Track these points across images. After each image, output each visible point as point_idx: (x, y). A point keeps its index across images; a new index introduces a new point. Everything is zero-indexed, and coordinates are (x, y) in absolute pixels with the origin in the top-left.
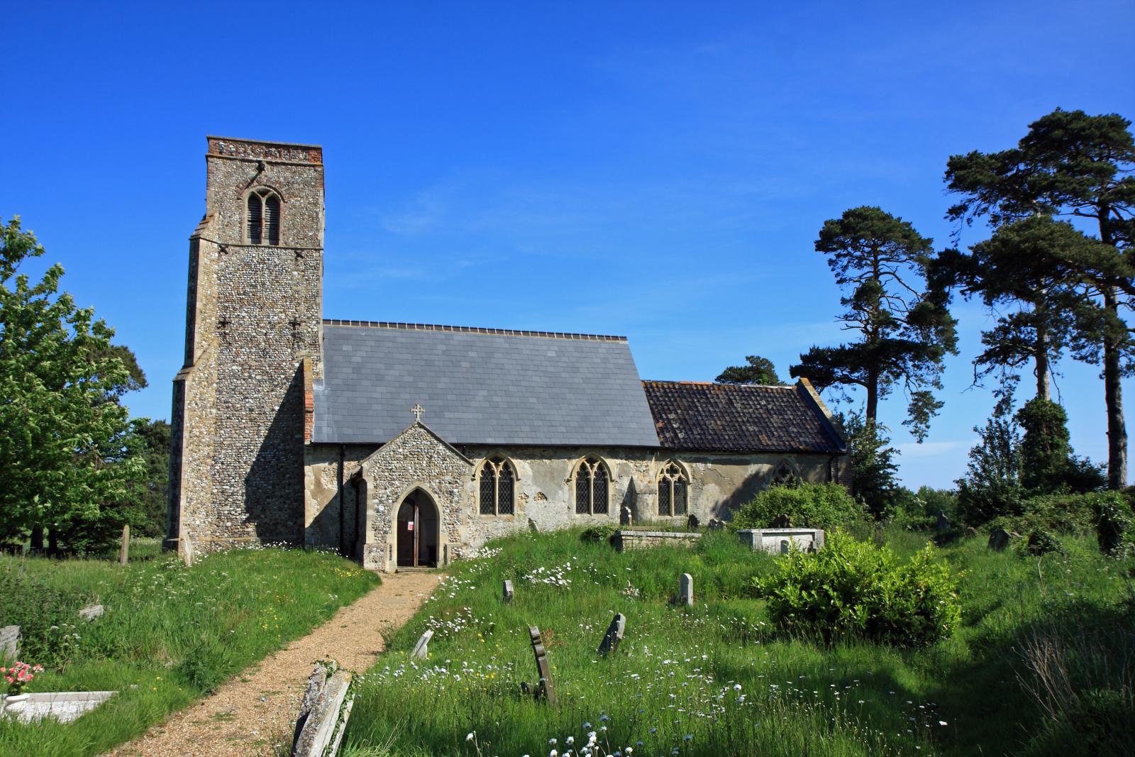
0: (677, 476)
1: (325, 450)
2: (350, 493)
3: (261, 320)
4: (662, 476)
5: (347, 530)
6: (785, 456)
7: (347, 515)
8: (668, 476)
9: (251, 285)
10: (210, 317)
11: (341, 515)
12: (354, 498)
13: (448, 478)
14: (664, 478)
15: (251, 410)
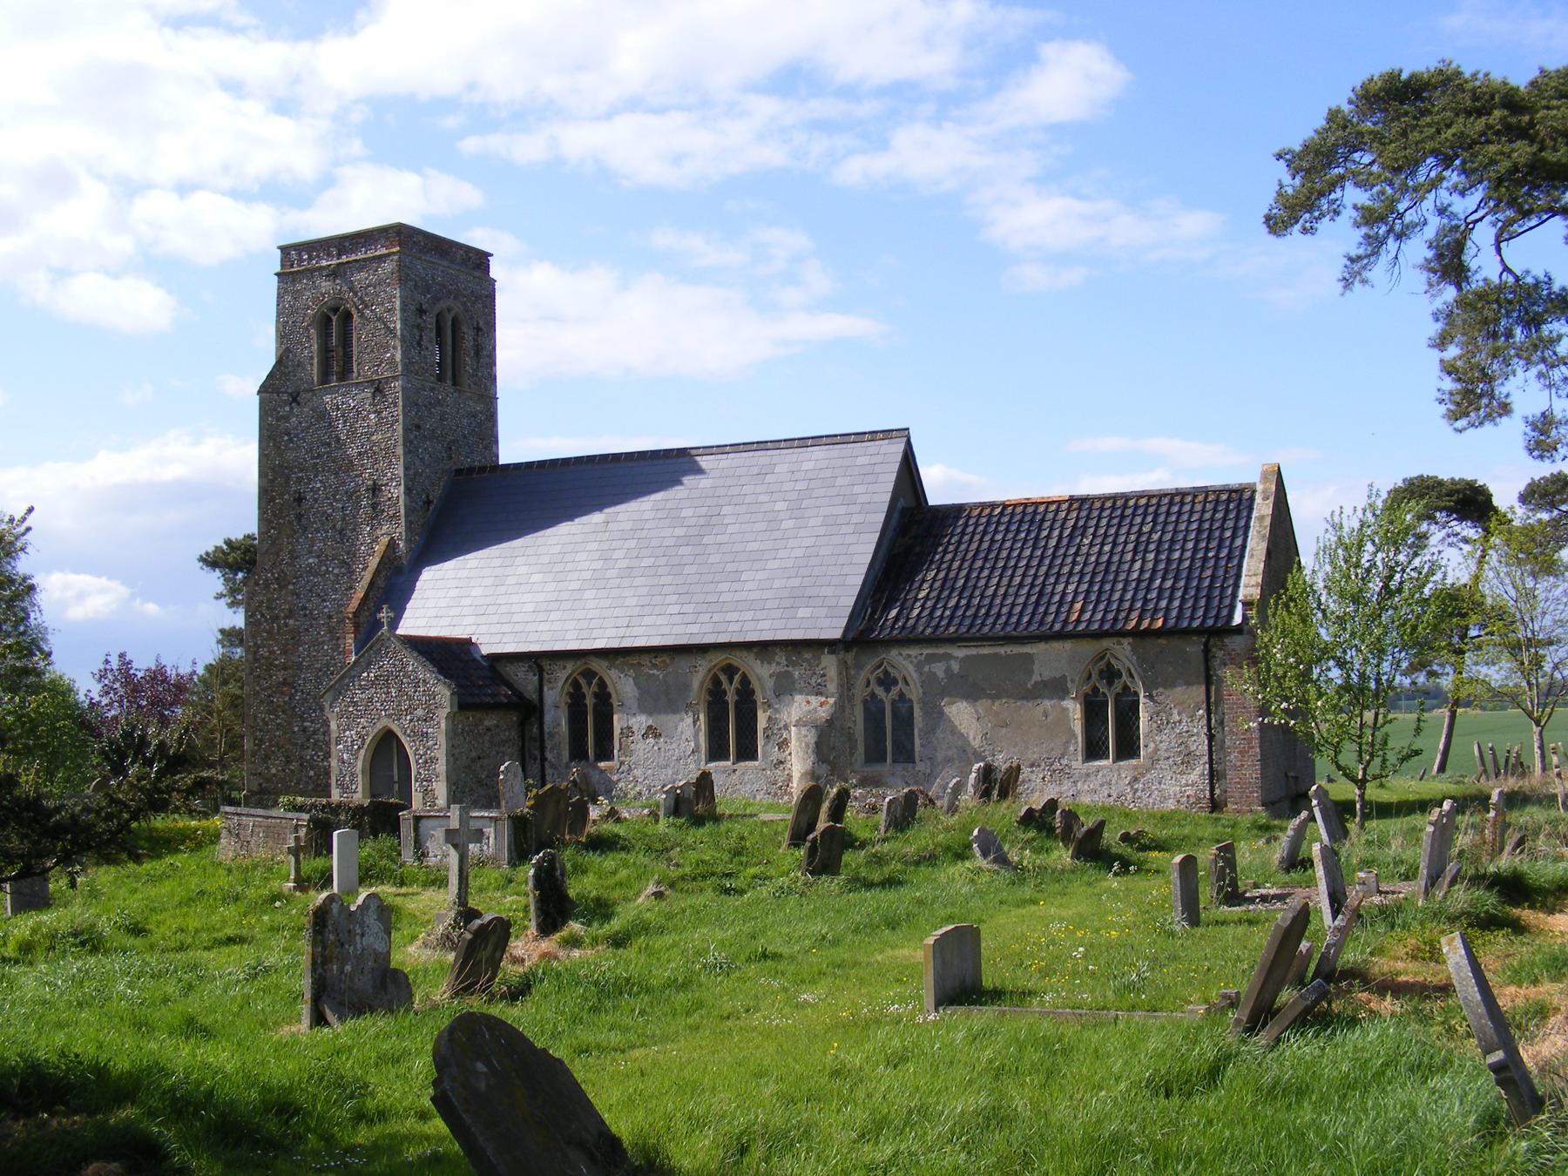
0: (895, 691)
3: (336, 492)
6: (1106, 643)
8: (880, 692)
10: (281, 495)
13: (420, 712)
15: (330, 617)
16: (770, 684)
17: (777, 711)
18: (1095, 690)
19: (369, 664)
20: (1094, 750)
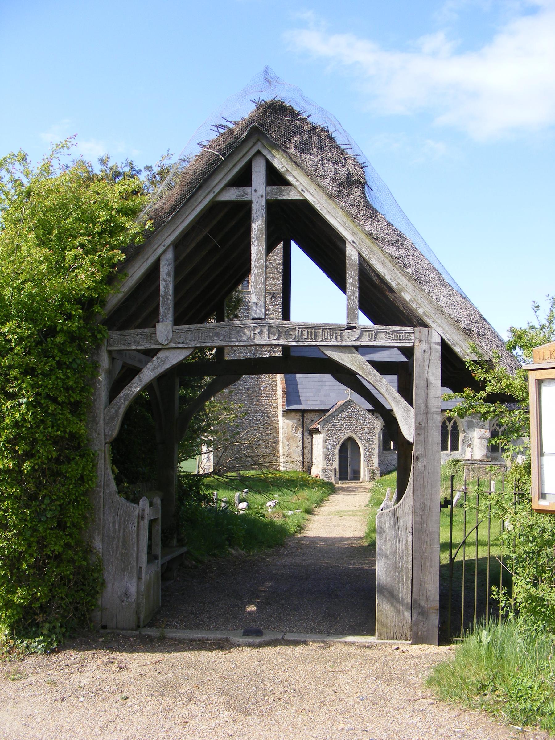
1: (293, 414)
2: (308, 438)
4: (494, 427)
5: (306, 460)
7: (306, 451)
8: (497, 428)
9: (246, 316)
11: (303, 451)
12: (310, 442)
13: (366, 430)
14: (495, 429)
15: (248, 390)
16: (465, 424)
17: (468, 434)
18: (495, 429)
19: (343, 411)
20: (444, 448)
